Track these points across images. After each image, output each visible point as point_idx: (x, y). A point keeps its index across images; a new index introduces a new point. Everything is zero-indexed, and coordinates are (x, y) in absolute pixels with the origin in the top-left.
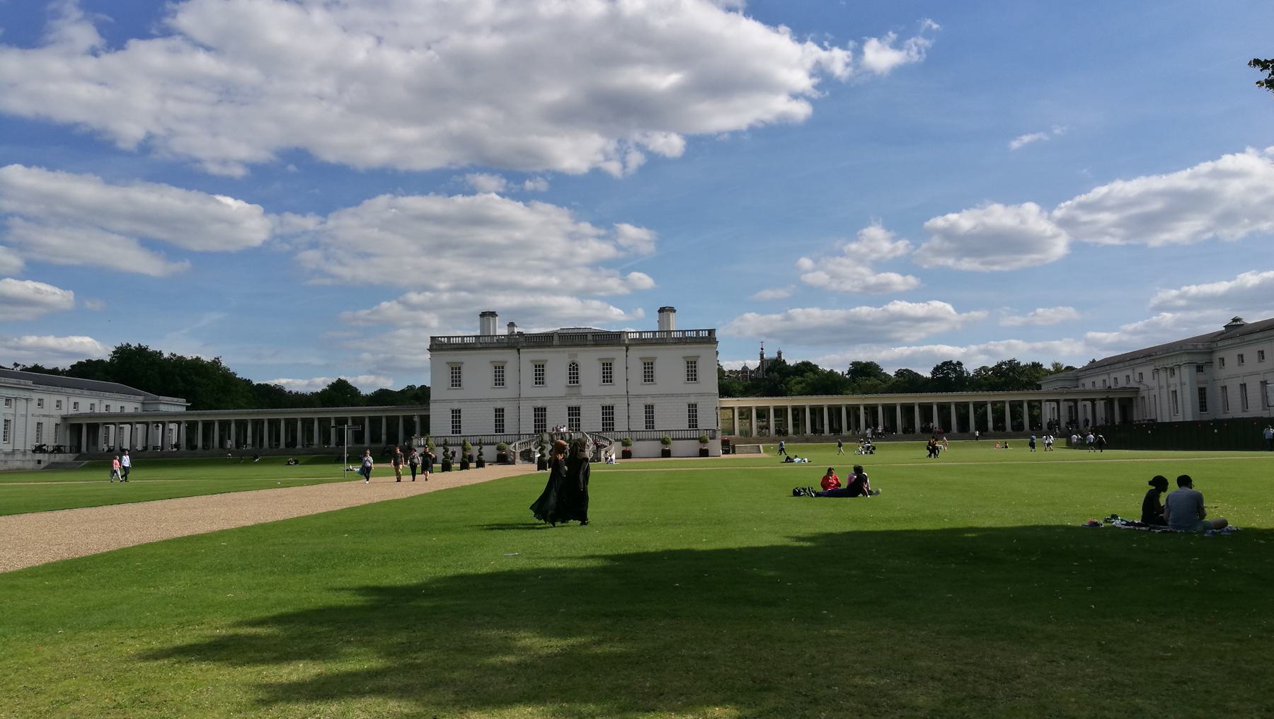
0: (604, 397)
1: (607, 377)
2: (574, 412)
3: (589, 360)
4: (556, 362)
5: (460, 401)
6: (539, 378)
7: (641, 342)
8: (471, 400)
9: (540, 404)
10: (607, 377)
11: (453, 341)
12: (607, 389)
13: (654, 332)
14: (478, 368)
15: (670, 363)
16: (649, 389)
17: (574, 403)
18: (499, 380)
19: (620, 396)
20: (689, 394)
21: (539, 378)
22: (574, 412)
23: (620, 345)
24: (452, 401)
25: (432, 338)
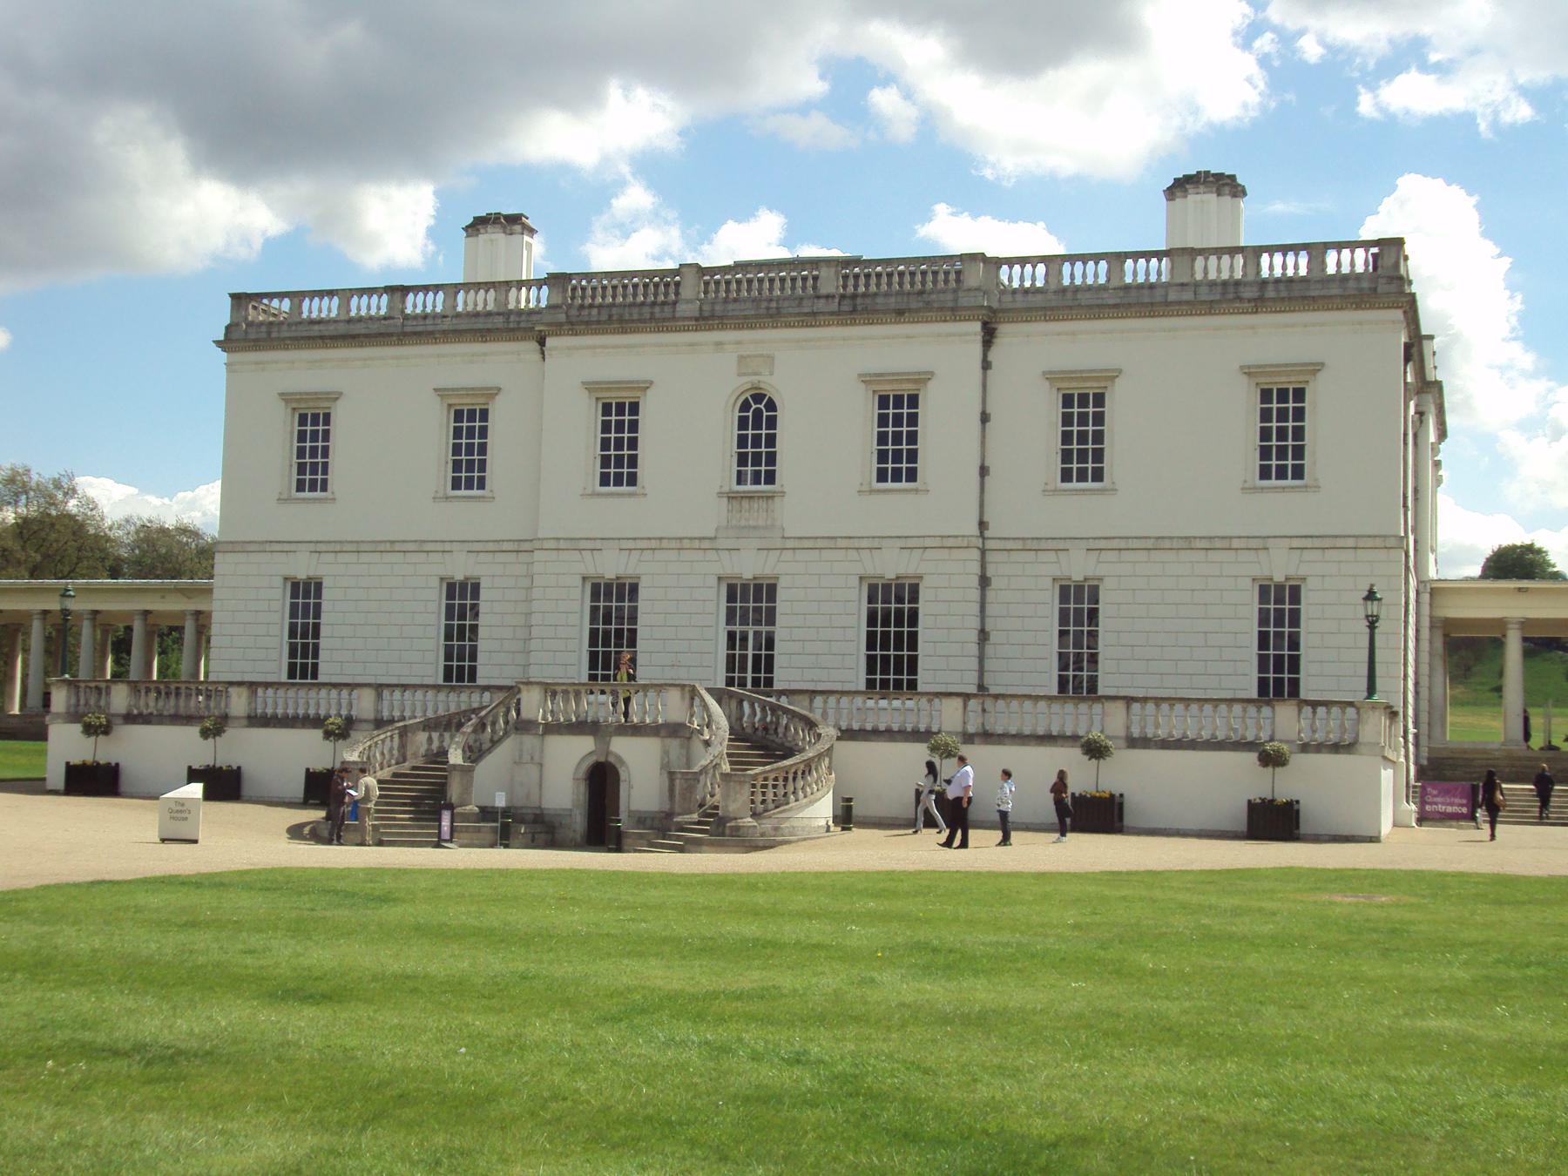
0: (875, 544)
1: (897, 457)
2: (751, 602)
3: (824, 383)
4: (689, 390)
5: (318, 547)
6: (619, 462)
7: (1061, 300)
8: (358, 548)
9: (611, 567)
10: (897, 457)
11: (313, 309)
12: (897, 509)
13: (452, 289)
14: (390, 411)
15: (1182, 398)
16: (1081, 511)
17: (749, 566)
18: (468, 465)
19: (947, 543)
20: (1260, 544)
21: (619, 462)
22: (751, 602)
23: (954, 312)
24: (285, 546)
25: (238, 299)
